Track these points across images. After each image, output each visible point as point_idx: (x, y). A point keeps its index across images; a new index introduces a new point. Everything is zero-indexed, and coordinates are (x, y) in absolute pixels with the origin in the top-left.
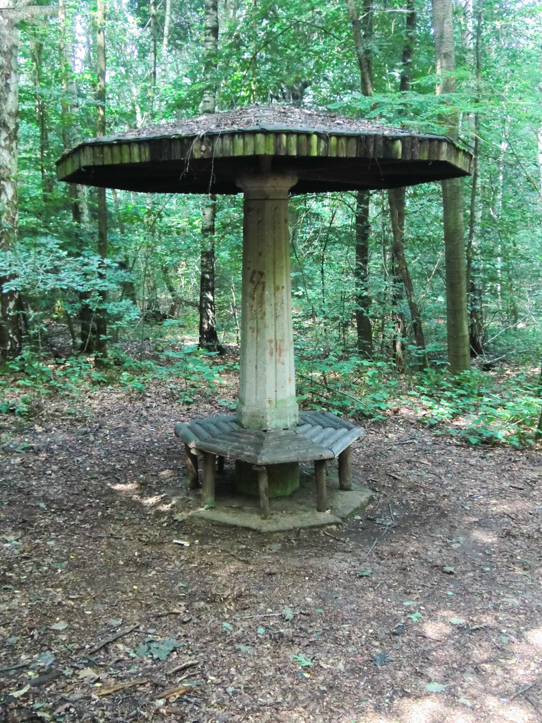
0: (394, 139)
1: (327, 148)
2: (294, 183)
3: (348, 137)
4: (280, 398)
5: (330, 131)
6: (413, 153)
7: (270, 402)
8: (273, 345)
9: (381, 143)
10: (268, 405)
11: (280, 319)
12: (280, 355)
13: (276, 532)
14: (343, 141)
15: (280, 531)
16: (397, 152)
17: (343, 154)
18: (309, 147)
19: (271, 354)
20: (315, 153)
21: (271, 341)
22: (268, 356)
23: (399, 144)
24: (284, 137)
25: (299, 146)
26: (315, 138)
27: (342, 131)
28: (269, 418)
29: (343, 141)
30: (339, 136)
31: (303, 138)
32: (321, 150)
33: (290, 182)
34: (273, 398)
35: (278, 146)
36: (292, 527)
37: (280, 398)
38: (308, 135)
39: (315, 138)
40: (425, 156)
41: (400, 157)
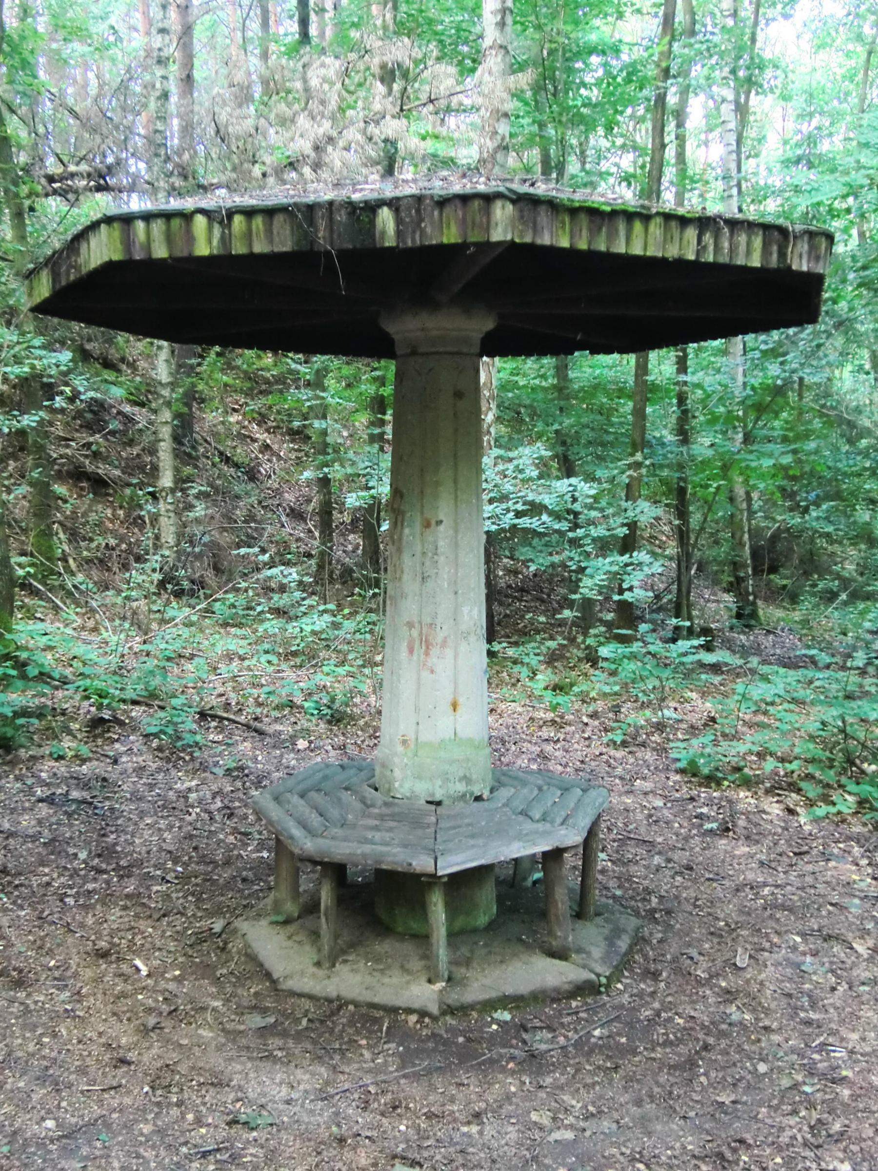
0: (372, 207)
1: (225, 240)
2: (489, 324)
3: (270, 212)
4: (423, 738)
5: (229, 204)
6: (423, 232)
7: (404, 742)
8: (415, 633)
9: (341, 217)
10: (400, 749)
11: (430, 584)
12: (427, 654)
13: (301, 995)
14: (258, 222)
15: (310, 997)
16: (383, 233)
17: (259, 248)
18: (190, 238)
19: (411, 651)
20: (202, 250)
21: (410, 625)
22: (404, 653)
23: (385, 216)
24: (140, 225)
25: (169, 239)
26: (200, 221)
27: (253, 202)
28: (397, 773)
29: (258, 222)
30: (249, 213)
31: (176, 223)
32: (215, 242)
33: (483, 324)
34: (411, 736)
35: (128, 242)
36: (334, 994)
37: (423, 738)
38: (187, 217)
39: (200, 221)
40: (451, 236)
41: (390, 242)
